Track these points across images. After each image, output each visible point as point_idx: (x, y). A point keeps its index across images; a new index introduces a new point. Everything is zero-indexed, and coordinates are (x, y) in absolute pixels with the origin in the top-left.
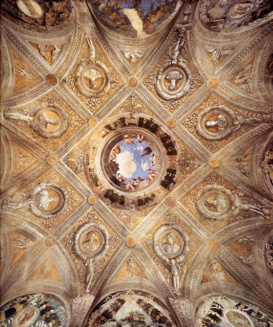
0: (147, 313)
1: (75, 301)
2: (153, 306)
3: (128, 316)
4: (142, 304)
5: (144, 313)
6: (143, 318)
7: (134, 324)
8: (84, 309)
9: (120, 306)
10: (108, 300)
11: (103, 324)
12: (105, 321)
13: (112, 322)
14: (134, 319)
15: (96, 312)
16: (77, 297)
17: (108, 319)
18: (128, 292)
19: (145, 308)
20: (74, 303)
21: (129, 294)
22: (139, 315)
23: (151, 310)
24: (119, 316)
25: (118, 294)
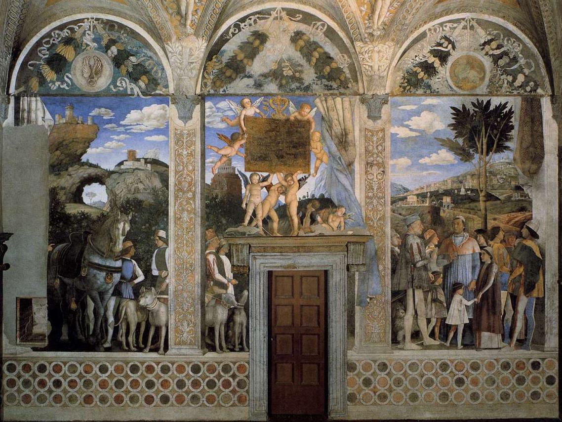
0: (309, 61)
1: (169, 47)
2: (321, 47)
3: (274, 67)
4: (301, 43)
5: (303, 62)
6: (301, 72)
7: (284, 82)
8: (192, 63)
9: (257, 48)
10: (234, 34)
11: (230, 83)
12: (233, 77)
13: (245, 80)
14: (284, 73)
15: (214, 60)
16: (170, 40)
17: (237, 74)
18: (274, 14)
19: (305, 50)
20: (170, 52)
21: (276, 18)
22: (294, 65)
23: (316, 55)
24: (257, 67)
25: (253, 20)
